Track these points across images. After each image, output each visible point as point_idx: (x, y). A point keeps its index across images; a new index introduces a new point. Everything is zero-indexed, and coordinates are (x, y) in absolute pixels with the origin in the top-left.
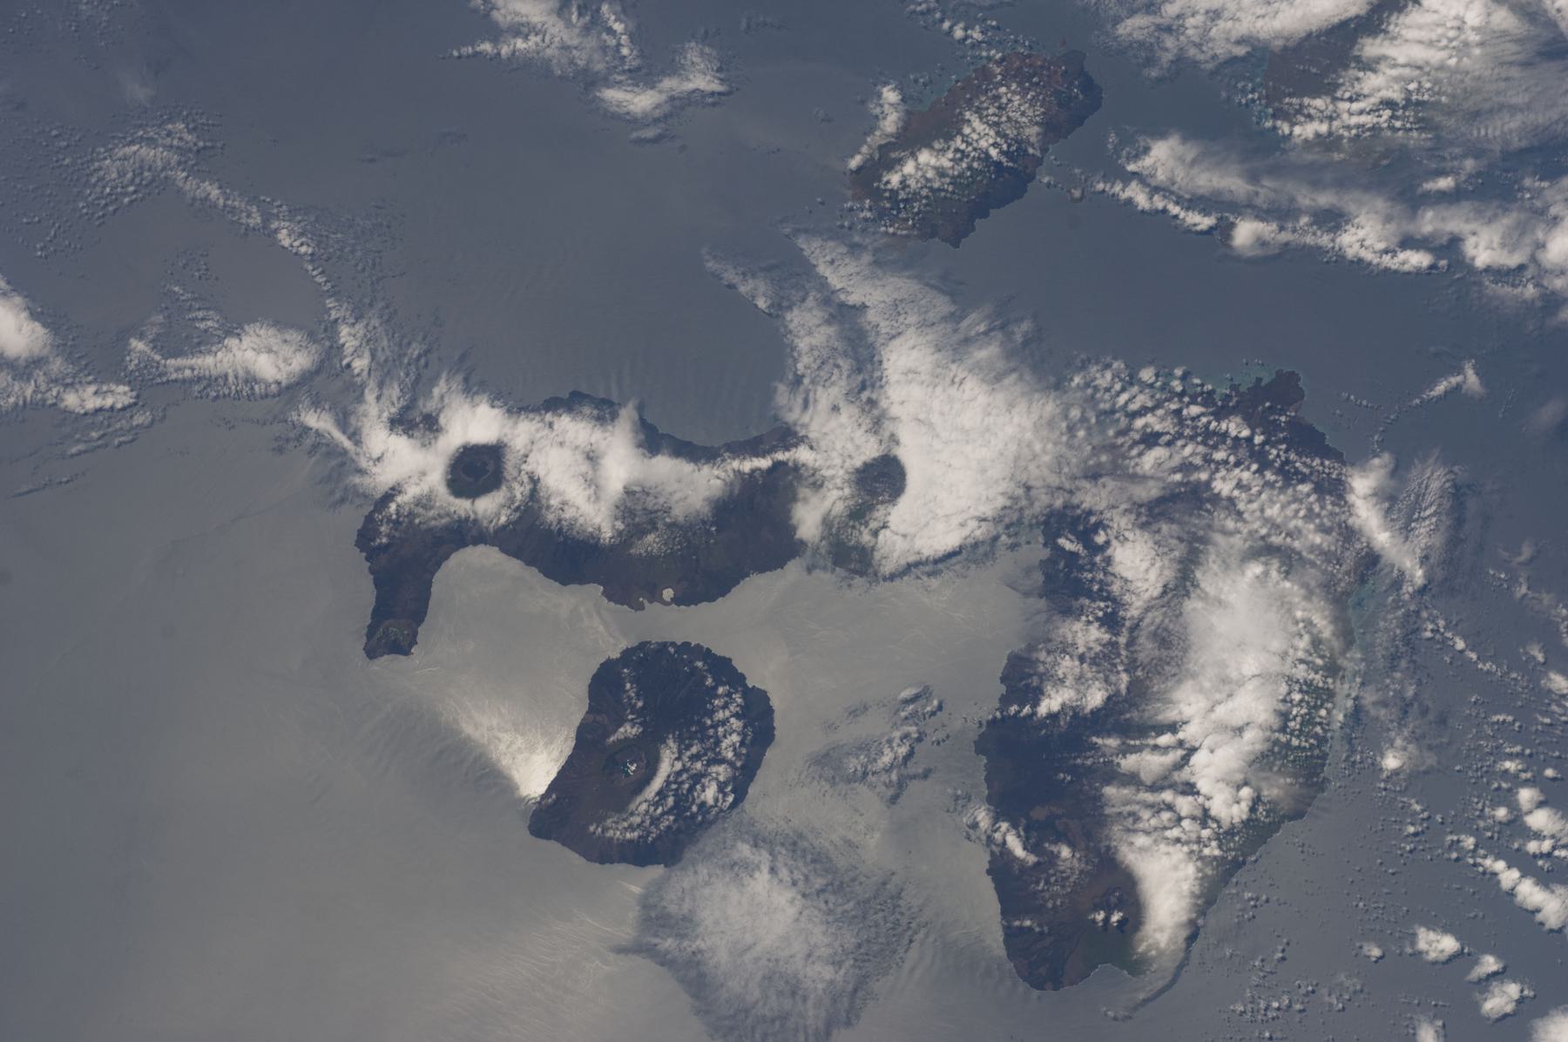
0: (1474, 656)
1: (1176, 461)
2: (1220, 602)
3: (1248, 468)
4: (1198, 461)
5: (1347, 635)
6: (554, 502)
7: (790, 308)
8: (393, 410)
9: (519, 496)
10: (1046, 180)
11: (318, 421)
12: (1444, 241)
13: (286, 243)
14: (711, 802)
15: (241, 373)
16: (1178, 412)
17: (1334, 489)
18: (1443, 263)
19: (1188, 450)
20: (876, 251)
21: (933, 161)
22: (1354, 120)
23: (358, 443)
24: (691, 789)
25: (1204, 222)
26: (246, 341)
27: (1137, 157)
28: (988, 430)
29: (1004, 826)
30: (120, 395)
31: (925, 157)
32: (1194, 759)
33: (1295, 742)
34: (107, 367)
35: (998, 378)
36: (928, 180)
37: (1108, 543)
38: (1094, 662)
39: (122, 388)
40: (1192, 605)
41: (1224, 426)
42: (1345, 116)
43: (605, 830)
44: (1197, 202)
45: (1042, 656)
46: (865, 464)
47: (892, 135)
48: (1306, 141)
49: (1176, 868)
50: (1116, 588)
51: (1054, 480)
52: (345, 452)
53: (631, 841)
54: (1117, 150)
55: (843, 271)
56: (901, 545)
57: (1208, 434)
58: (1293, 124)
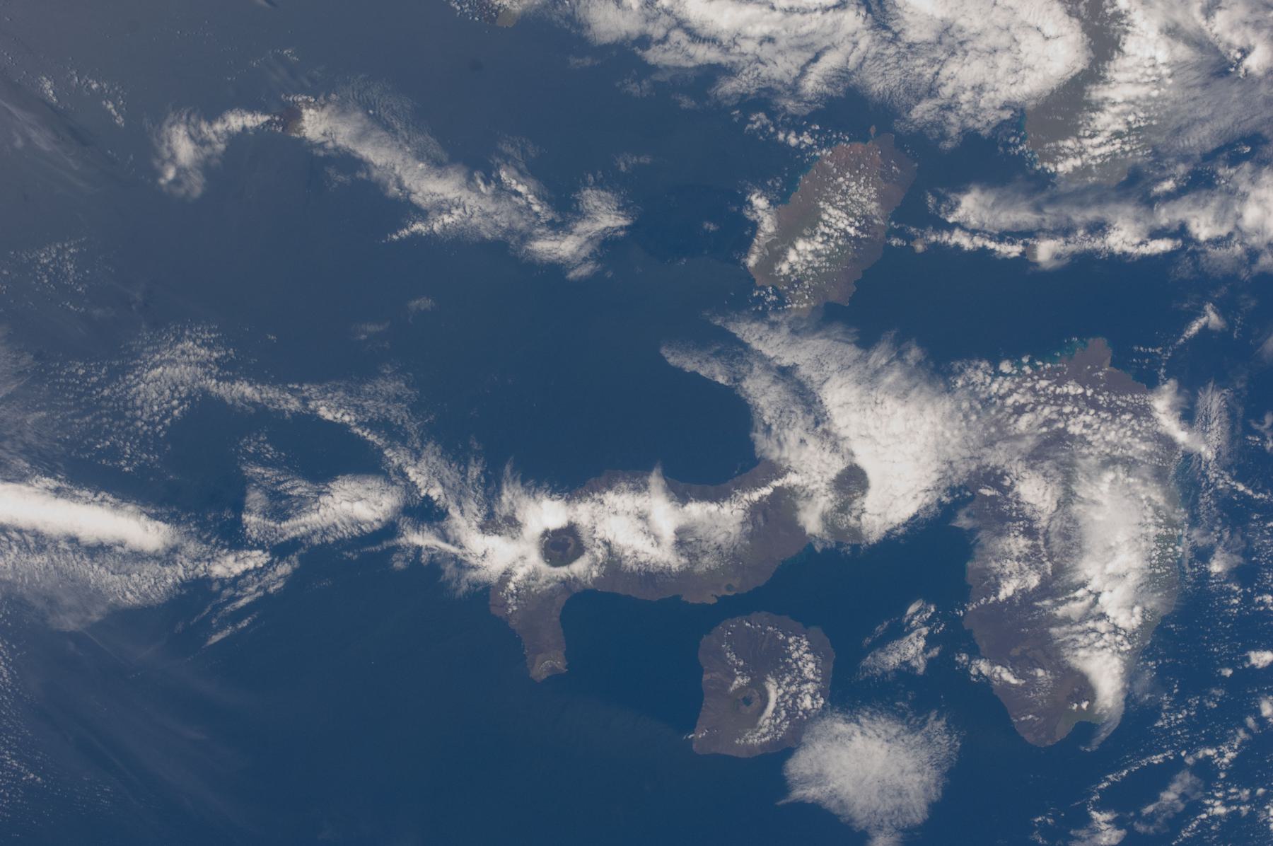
1: (1041, 419)
2: (1095, 503)
3: (1088, 413)
4: (1055, 416)
5: (1170, 499)
7: (743, 378)
8: (478, 519)
9: (600, 556)
10: (894, 242)
11: (422, 539)
12: (1176, 227)
13: (329, 416)
15: (345, 520)
16: (1032, 389)
17: (1143, 412)
18: (1179, 242)
19: (1047, 411)
20: (790, 324)
21: (809, 247)
23: (461, 547)
24: (795, 703)
25: (1014, 250)
26: (337, 497)
27: (952, 209)
28: (911, 431)
29: (998, 668)
30: (257, 558)
31: (801, 245)
32: (1101, 600)
33: (1158, 571)
34: (235, 539)
35: (906, 394)
36: (809, 262)
37: (1012, 483)
38: (1027, 558)
40: (1076, 508)
41: (1065, 390)
42: (1090, 150)
43: (746, 740)
44: (1002, 236)
45: (993, 564)
46: (838, 476)
47: (770, 235)
48: (1067, 174)
49: (1107, 662)
50: (1028, 510)
51: (966, 453)
52: (455, 557)
53: (766, 742)
54: (937, 208)
55: (771, 344)
56: (878, 521)
57: (1056, 397)
58: (1056, 164)
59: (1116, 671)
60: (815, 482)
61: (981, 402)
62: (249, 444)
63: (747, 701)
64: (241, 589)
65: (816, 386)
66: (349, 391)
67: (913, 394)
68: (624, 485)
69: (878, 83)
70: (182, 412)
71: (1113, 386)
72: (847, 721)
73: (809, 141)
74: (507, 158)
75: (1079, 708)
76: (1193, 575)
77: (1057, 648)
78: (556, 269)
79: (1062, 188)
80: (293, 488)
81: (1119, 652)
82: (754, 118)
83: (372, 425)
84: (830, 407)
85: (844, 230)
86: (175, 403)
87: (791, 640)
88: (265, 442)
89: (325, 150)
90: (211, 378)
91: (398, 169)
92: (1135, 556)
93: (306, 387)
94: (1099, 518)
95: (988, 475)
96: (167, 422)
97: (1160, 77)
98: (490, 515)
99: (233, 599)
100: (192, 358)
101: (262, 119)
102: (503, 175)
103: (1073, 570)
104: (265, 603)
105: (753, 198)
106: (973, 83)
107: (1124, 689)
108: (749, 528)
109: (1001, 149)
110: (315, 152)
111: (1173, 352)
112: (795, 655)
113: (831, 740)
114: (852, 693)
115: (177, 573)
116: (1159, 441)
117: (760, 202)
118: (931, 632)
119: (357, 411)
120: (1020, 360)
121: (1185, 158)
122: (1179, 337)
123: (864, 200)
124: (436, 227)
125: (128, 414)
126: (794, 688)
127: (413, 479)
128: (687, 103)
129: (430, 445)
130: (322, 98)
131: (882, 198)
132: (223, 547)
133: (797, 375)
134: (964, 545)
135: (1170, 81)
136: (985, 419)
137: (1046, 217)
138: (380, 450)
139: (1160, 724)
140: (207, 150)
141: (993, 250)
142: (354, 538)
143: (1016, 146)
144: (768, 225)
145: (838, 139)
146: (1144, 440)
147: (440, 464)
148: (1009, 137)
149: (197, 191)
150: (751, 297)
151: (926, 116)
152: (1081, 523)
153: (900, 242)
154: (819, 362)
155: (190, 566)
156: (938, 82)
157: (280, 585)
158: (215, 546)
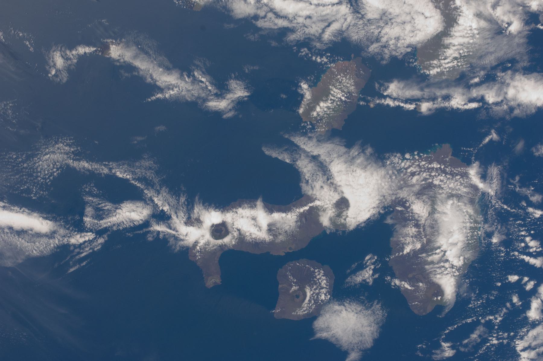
0: (509, 209)
1: (422, 178)
2: (444, 213)
4: (428, 177)
5: (476, 211)
6: (247, 234)
7: (297, 160)
9: (236, 235)
10: (361, 103)
11: (160, 228)
12: (480, 98)
13: (121, 176)
14: (324, 299)
15: (127, 220)
16: (419, 165)
17: (465, 175)
18: (481, 104)
19: (424, 175)
20: (317, 137)
21: (325, 105)
22: (447, 66)
23: (177, 231)
24: (317, 297)
25: (412, 107)
26: (124, 210)
27: (386, 89)
28: (368, 183)
29: (403, 283)
30: (90, 236)
31: (322, 104)
32: (446, 254)
33: (470, 242)
34: (80, 228)
35: (365, 167)
36: (325, 111)
37: (410, 205)
38: (416, 237)
39: (89, 234)
40: (436, 216)
41: (432, 166)
42: (444, 65)
43: (297, 313)
44: (407, 101)
45: (402, 239)
47: (309, 100)
48: (434, 75)
49: (449, 280)
50: (416, 216)
51: (391, 192)
52: (174, 236)
54: (379, 89)
55: (309, 146)
58: (429, 71)
59: (452, 284)
60: (327, 204)
61: (397, 171)
62: (87, 188)
63: (297, 297)
64: (83, 249)
65: (327, 164)
66: (129, 165)
67: (369, 167)
68: (246, 205)
69: (355, 36)
70: (58, 174)
71: (453, 164)
72: (340, 305)
73: (326, 60)
74: (197, 66)
75: (437, 299)
76: (485, 243)
77: (428, 274)
78: (218, 114)
79: (432, 81)
80: (105, 206)
81: (454, 276)
82: (302, 50)
83: (139, 180)
84: (333, 173)
85: (340, 98)
86: (55, 170)
87: (316, 271)
88: (93, 187)
89: (120, 63)
90: (70, 159)
91: (151, 71)
92: (461, 235)
93: (111, 163)
94: (446, 219)
95: (399, 201)
96: (51, 178)
97: (474, 34)
98: (189, 218)
99: (79, 253)
100: (62, 151)
101: (93, 49)
102: (196, 74)
103: (435, 241)
104: (93, 255)
105: (302, 84)
106: (395, 36)
107: (456, 291)
108: (299, 223)
109: (407, 64)
110: (115, 63)
111: (478, 150)
112: (318, 277)
113: (333, 313)
114: (342, 293)
115: (55, 242)
116: (471, 187)
117: (305, 86)
118: (375, 267)
119: (132, 174)
120: (413, 152)
121: (483, 68)
122: (480, 144)
123: (349, 85)
124: (167, 96)
125: (35, 174)
126: (317, 291)
127: (156, 203)
128: (274, 44)
129: (164, 188)
130: (118, 40)
131: (356, 84)
132: (75, 231)
133: (320, 159)
134: (389, 231)
135: (478, 36)
136: (399, 178)
137: (425, 93)
138: (142, 190)
139: (471, 306)
140: (69, 62)
141: (403, 107)
142: (131, 227)
143: (413, 63)
144: (308, 96)
145: (338, 60)
146: (465, 187)
147: (168, 196)
148: (410, 59)
149: (65, 79)
150: (300, 126)
151: (375, 50)
152: (439, 222)
153: (364, 103)
154: (329, 154)
155: (61, 239)
156: (380, 36)
157: (99, 247)
158: (72, 231)
